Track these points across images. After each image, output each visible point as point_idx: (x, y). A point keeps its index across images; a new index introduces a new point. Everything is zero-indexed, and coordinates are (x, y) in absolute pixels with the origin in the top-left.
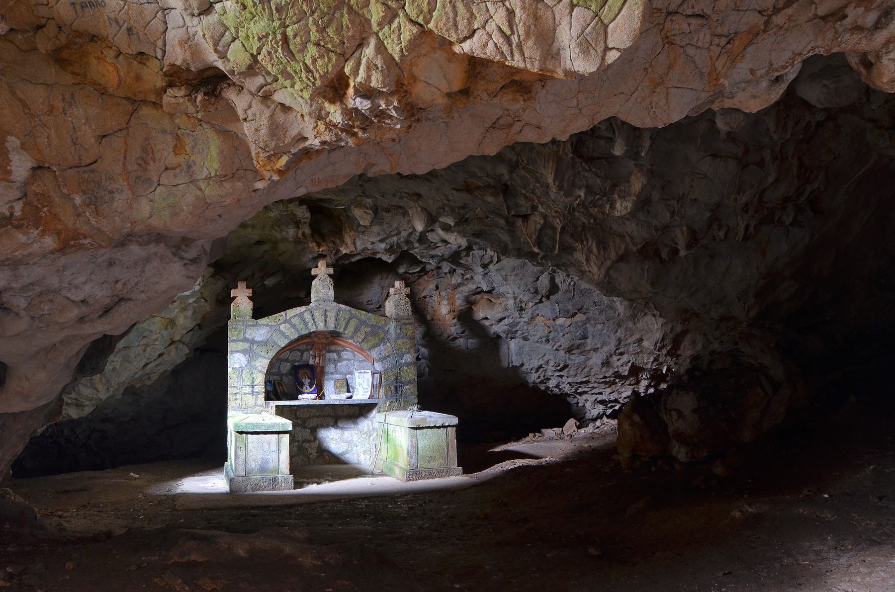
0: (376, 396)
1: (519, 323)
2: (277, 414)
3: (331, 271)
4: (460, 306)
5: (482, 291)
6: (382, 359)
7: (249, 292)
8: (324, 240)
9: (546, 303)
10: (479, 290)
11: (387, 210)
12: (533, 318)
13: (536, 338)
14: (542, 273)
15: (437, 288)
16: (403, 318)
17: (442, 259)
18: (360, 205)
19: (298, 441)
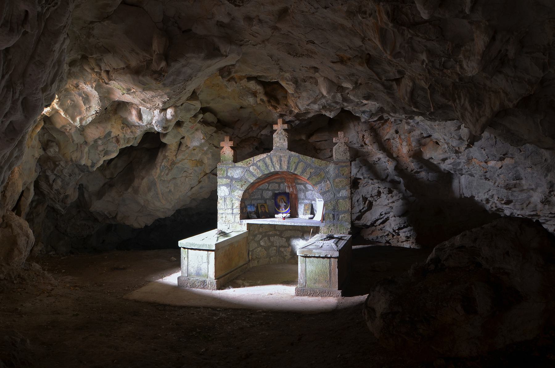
3: (286, 126)
7: (231, 144)
8: (278, 104)
18: (283, 79)
19: (276, 246)
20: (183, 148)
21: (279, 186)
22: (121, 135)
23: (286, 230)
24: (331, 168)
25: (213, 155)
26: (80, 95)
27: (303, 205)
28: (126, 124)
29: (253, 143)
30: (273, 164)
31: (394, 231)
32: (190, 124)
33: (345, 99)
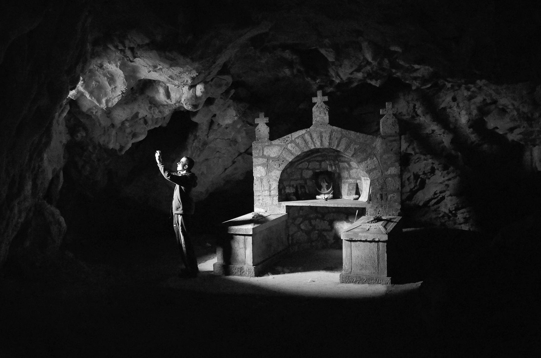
3: (326, 98)
7: (266, 120)
16: (390, 136)
19: (318, 230)
20: (215, 127)
21: (320, 165)
22: (149, 116)
23: (329, 212)
24: (378, 143)
25: (247, 134)
26: (105, 75)
27: (347, 185)
28: (154, 104)
31: (450, 212)
32: (222, 101)
33: (394, 65)
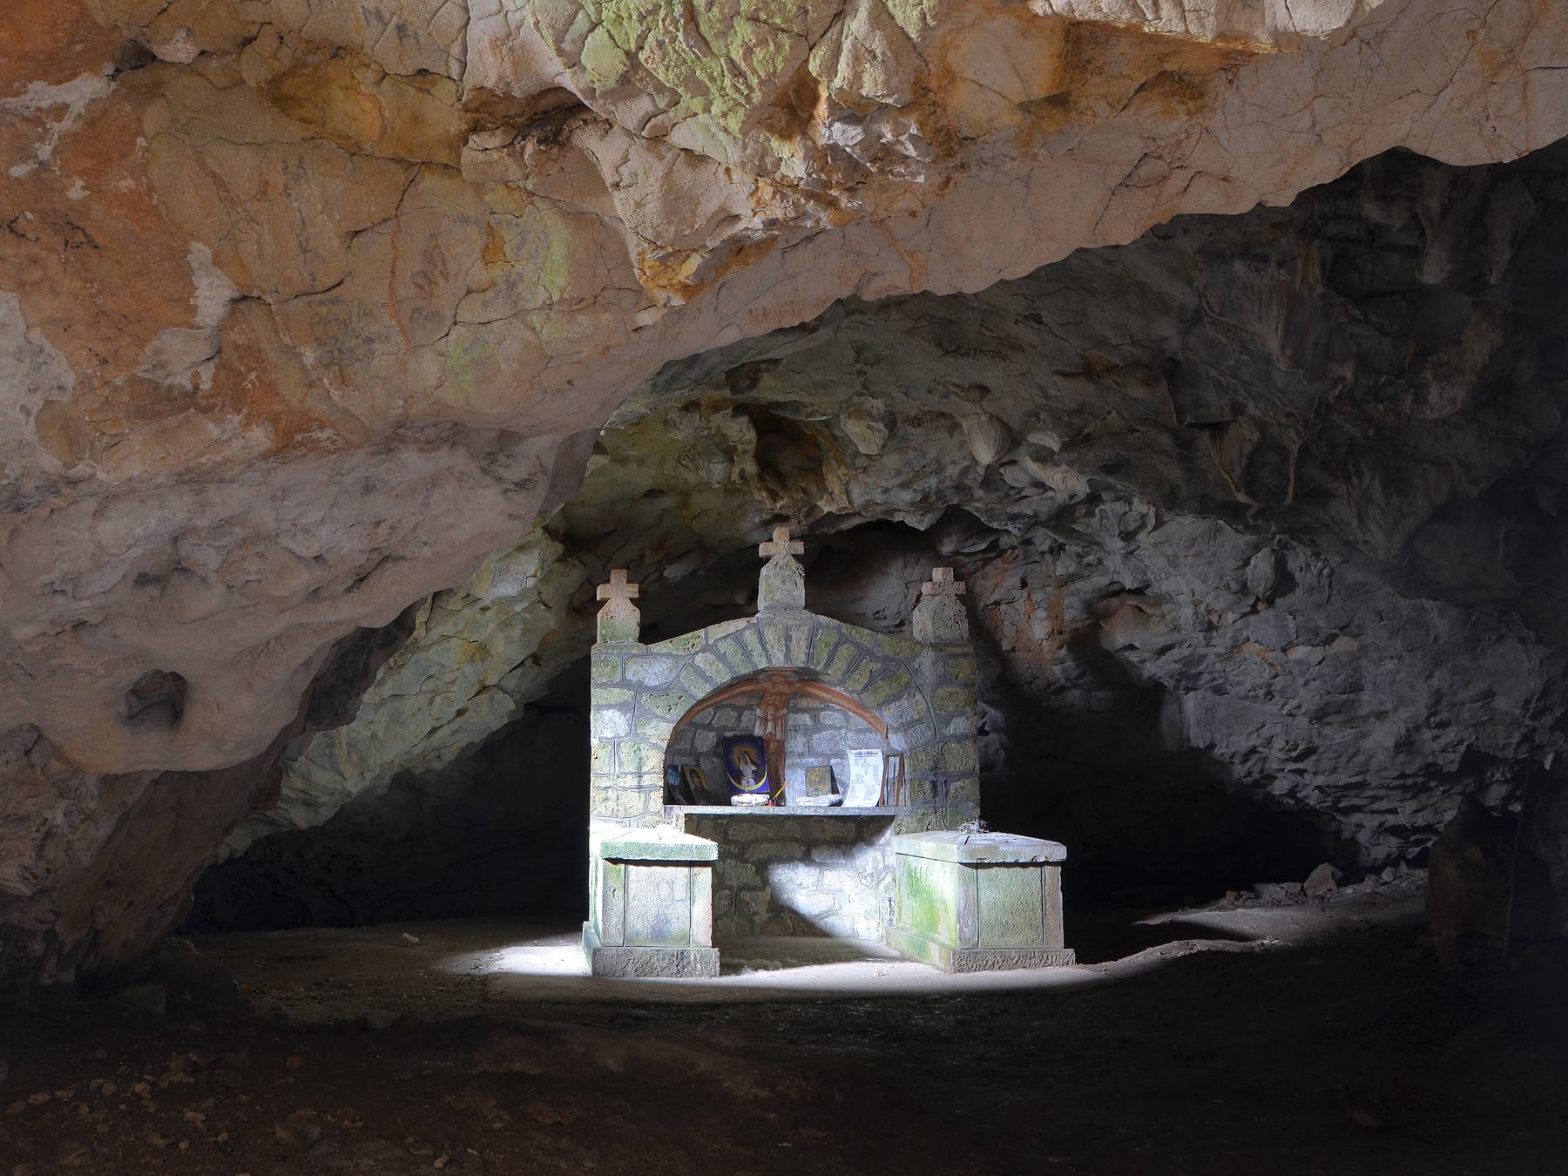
0: (892, 801)
1: (1204, 656)
2: (687, 831)
4: (1073, 620)
5: (1123, 590)
6: (906, 727)
9: (1266, 613)
10: (1115, 587)
11: (916, 422)
12: (1235, 647)
13: (1242, 690)
14: (1257, 549)
15: (1024, 584)
16: (951, 644)
17: (1035, 522)
29: (697, 587)
30: (764, 649)
